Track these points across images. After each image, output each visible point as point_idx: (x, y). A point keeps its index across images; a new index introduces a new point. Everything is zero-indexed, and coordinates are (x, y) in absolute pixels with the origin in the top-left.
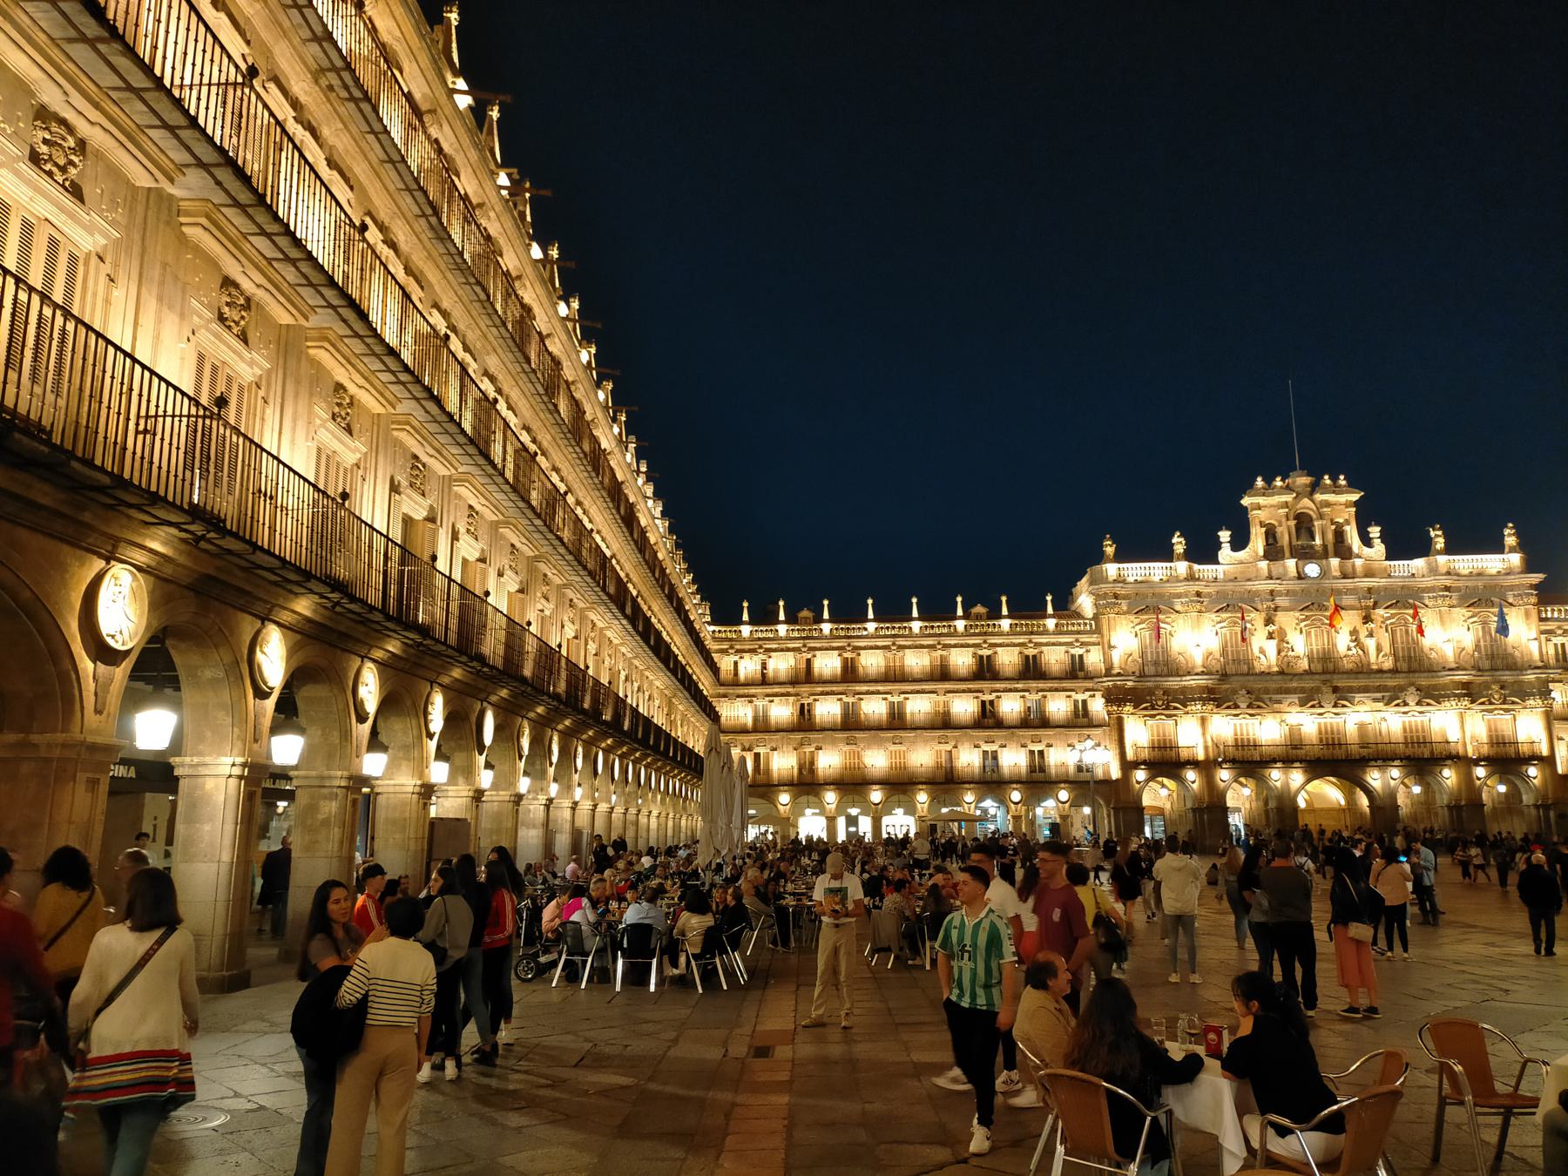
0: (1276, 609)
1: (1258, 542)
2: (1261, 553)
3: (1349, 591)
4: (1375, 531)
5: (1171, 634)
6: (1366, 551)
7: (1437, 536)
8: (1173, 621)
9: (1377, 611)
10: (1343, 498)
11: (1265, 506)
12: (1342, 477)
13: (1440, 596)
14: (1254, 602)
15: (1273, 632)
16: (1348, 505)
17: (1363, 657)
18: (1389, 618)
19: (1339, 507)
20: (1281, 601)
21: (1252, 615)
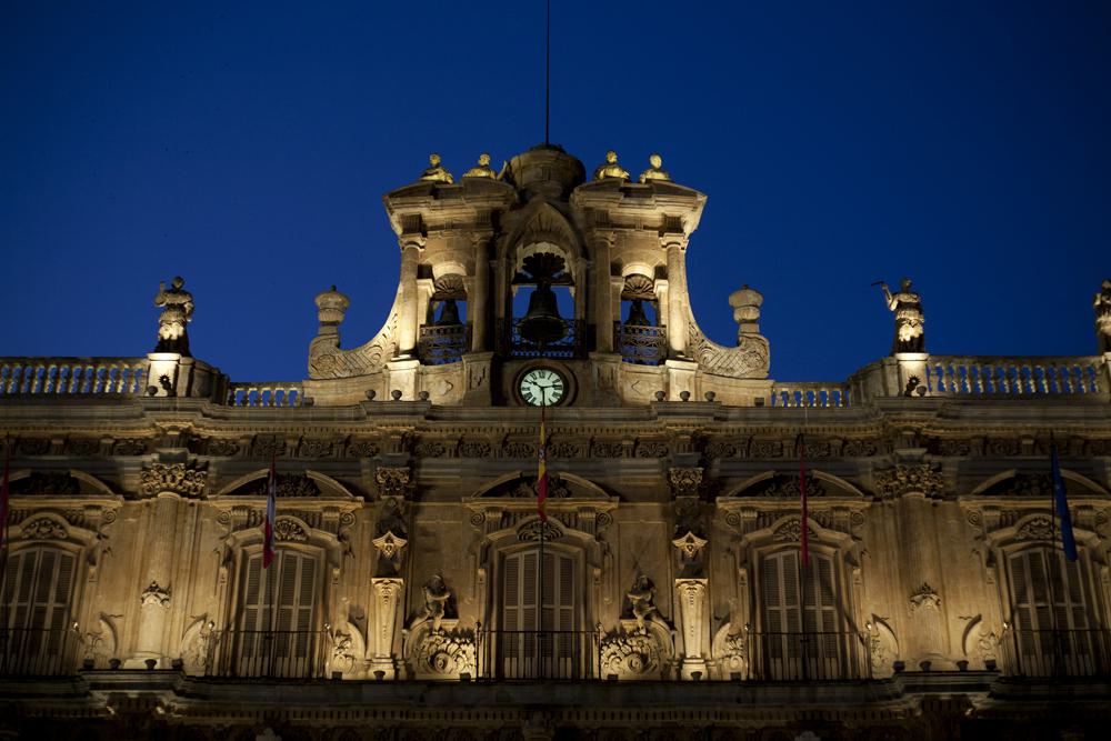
0: (418, 492)
1: (402, 326)
2: (407, 344)
3: (638, 448)
4: (746, 307)
5: (91, 560)
6: (715, 354)
7: (901, 306)
8: (107, 521)
9: (725, 504)
10: (654, 212)
11: (440, 228)
12: (656, 161)
13: (902, 460)
14: (357, 473)
15: (394, 557)
16: (673, 225)
17: (666, 639)
18: (755, 526)
19: (641, 234)
20: (436, 470)
21: (351, 507)
